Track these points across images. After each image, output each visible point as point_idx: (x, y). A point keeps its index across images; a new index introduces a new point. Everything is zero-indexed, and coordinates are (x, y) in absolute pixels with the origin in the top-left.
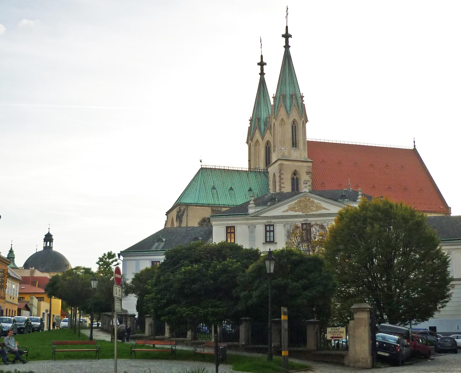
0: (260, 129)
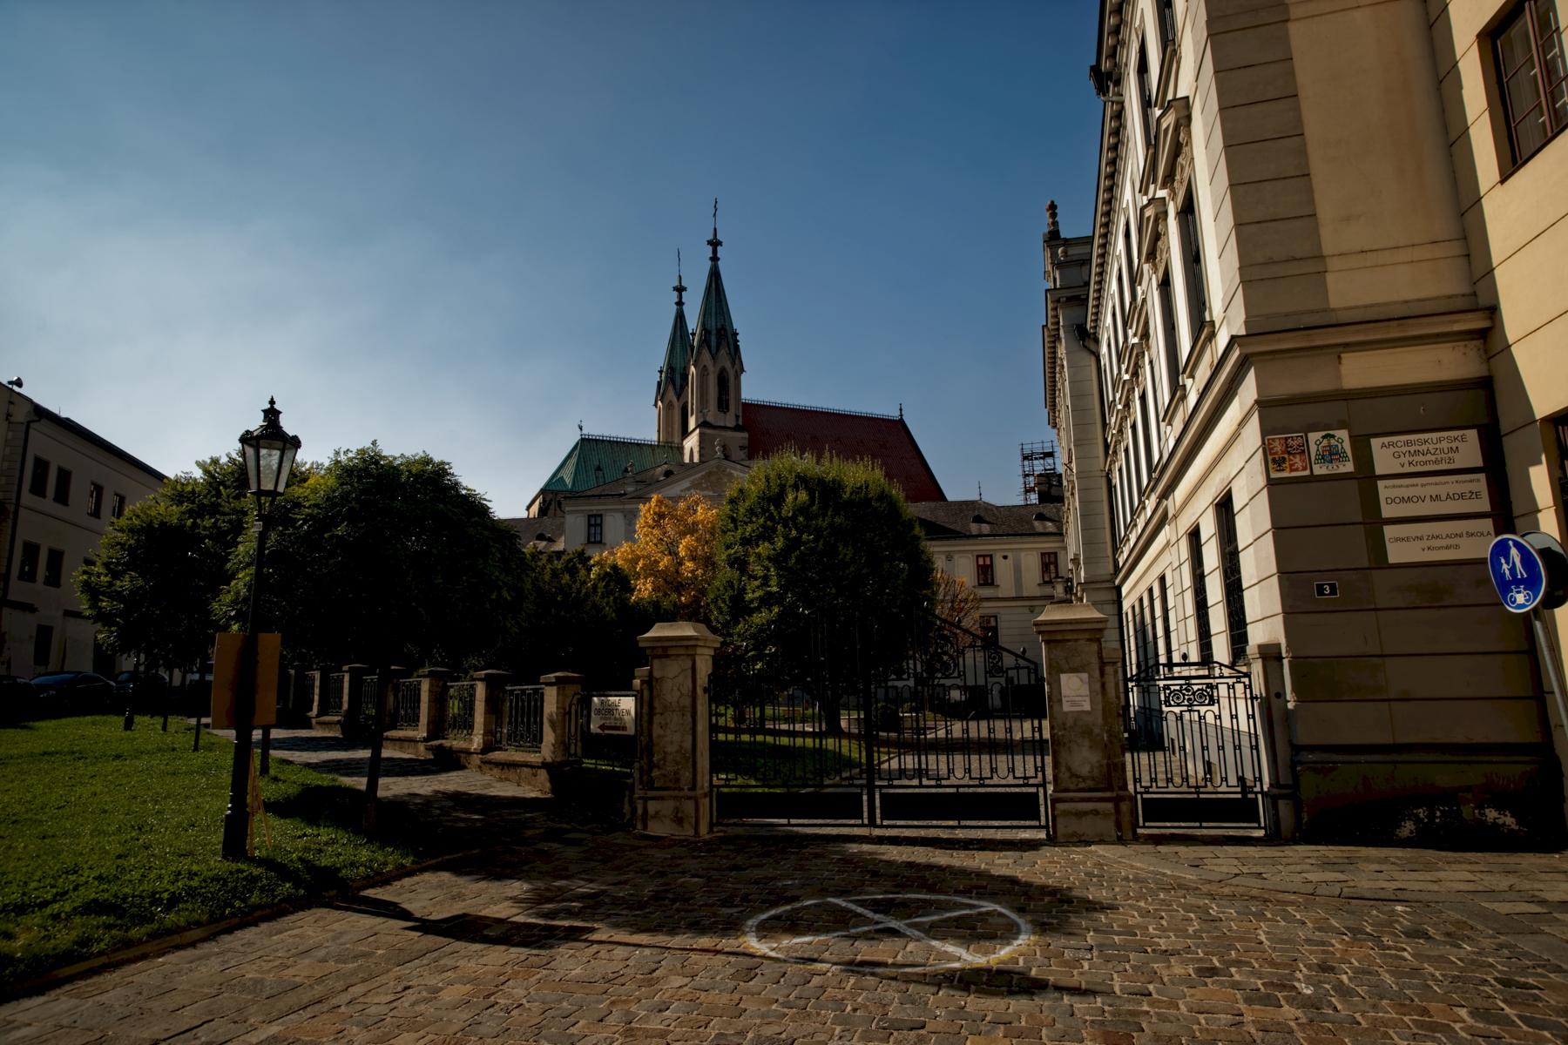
0: (674, 385)
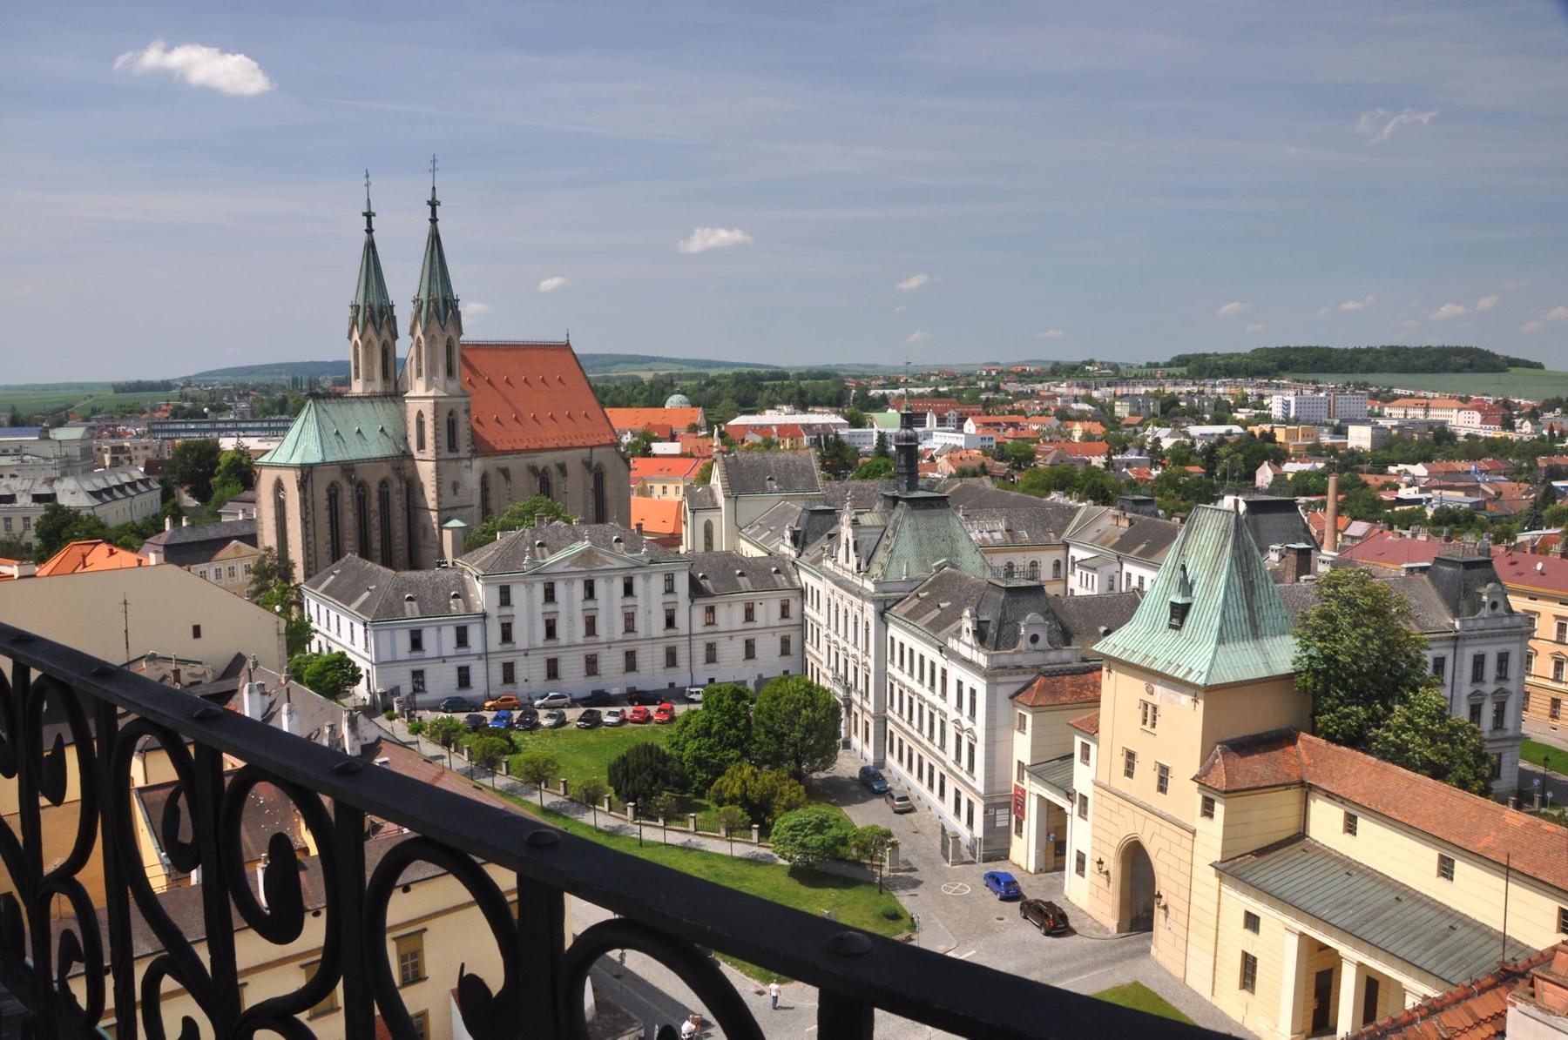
0: (374, 323)
